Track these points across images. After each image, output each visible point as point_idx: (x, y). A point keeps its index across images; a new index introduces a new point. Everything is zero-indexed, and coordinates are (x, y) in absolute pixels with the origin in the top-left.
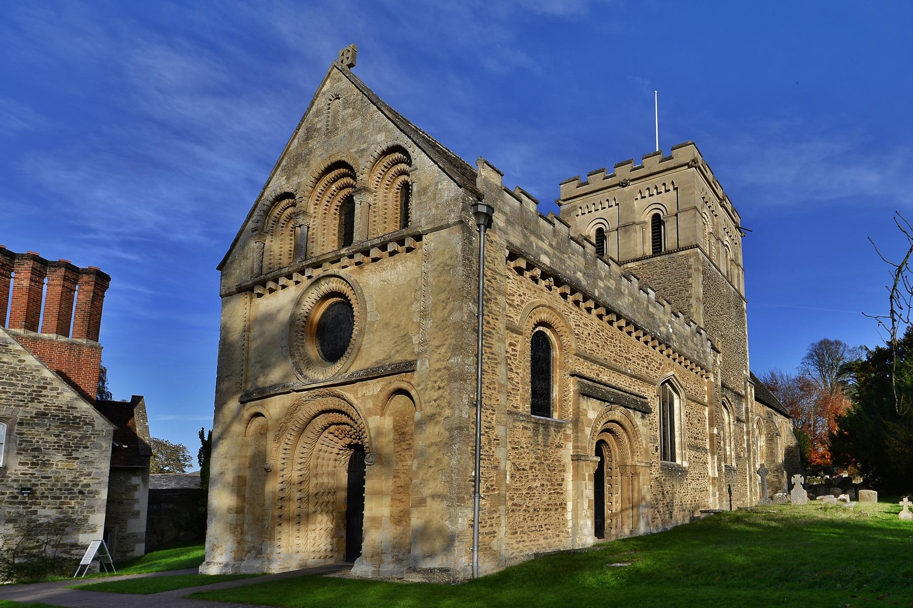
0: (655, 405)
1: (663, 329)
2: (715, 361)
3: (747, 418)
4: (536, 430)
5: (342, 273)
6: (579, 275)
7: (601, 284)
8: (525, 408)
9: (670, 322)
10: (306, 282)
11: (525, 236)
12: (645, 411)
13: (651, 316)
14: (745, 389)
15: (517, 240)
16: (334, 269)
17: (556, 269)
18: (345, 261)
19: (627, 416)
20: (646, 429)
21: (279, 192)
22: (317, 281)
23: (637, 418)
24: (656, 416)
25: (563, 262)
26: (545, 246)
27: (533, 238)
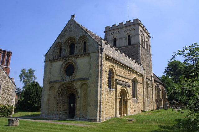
0: (131, 84)
1: (133, 66)
2: (144, 72)
3: (152, 86)
4: (109, 92)
5: (72, 59)
6: (117, 57)
7: (121, 58)
8: (107, 87)
9: (134, 64)
10: (64, 61)
11: (108, 52)
12: (129, 87)
13: (131, 64)
14: (152, 78)
15: (107, 53)
16: (71, 59)
17: (113, 57)
18: (73, 57)
19: (126, 88)
20: (130, 90)
21: (58, 42)
22: (67, 61)
23: (128, 88)
24: (131, 87)
25: (114, 55)
26: (111, 53)
27: (110, 52)
